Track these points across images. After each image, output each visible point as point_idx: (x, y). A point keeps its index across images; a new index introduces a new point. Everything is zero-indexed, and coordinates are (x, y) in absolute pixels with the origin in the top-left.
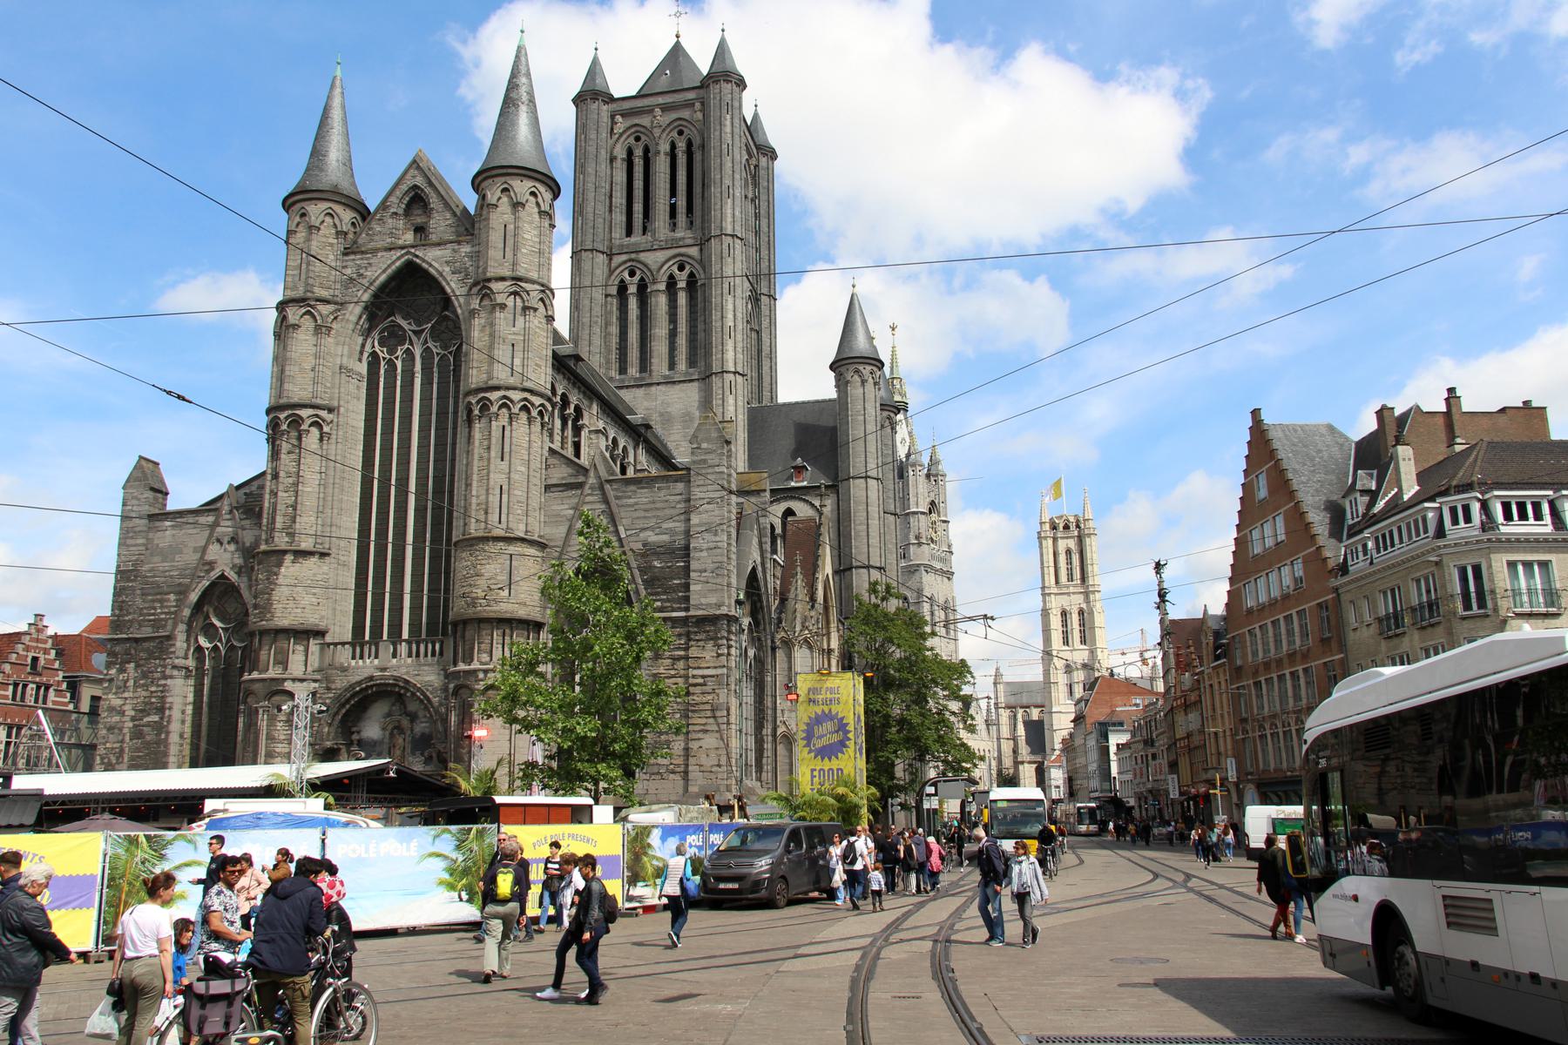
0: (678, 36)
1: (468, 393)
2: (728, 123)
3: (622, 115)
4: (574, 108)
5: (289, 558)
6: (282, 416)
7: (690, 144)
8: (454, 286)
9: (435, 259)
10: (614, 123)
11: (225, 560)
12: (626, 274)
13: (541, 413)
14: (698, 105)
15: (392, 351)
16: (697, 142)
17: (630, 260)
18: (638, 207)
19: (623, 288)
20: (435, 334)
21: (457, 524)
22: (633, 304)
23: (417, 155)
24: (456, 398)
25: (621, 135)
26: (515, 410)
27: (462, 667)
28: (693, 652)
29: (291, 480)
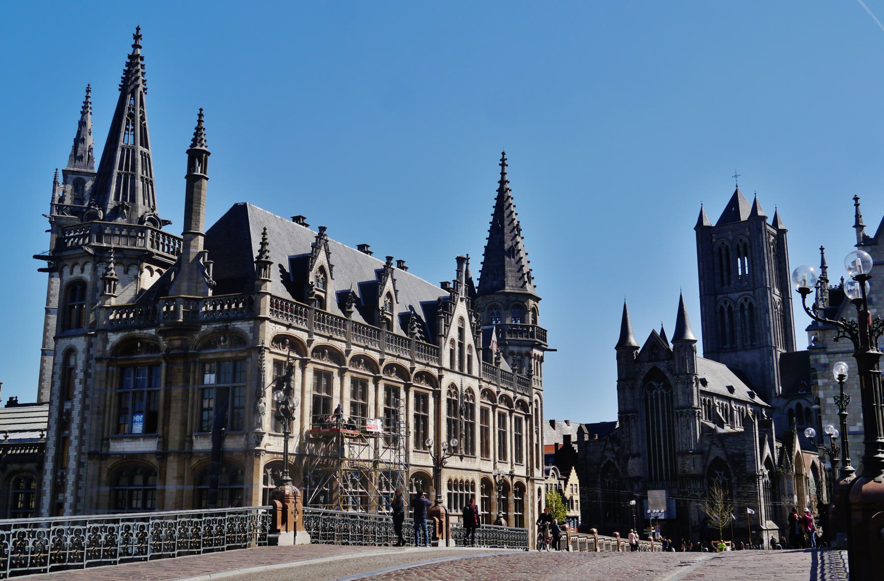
0: (737, 186)
1: (676, 409)
2: (760, 238)
3: (715, 234)
4: (695, 231)
5: (630, 458)
6: (624, 415)
7: (745, 245)
8: (668, 375)
9: (662, 366)
10: (712, 238)
11: (609, 456)
12: (723, 303)
13: (698, 414)
14: (747, 229)
15: (651, 392)
16: (748, 244)
17: (724, 297)
18: (725, 273)
19: (722, 309)
20: (664, 387)
21: (677, 447)
22: (726, 316)
23: (653, 331)
24: (672, 409)
25: (716, 242)
26: (691, 414)
27: (682, 490)
28: (749, 486)
29: (628, 435)
